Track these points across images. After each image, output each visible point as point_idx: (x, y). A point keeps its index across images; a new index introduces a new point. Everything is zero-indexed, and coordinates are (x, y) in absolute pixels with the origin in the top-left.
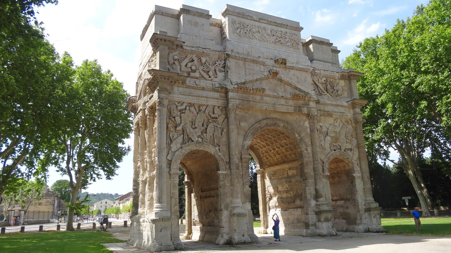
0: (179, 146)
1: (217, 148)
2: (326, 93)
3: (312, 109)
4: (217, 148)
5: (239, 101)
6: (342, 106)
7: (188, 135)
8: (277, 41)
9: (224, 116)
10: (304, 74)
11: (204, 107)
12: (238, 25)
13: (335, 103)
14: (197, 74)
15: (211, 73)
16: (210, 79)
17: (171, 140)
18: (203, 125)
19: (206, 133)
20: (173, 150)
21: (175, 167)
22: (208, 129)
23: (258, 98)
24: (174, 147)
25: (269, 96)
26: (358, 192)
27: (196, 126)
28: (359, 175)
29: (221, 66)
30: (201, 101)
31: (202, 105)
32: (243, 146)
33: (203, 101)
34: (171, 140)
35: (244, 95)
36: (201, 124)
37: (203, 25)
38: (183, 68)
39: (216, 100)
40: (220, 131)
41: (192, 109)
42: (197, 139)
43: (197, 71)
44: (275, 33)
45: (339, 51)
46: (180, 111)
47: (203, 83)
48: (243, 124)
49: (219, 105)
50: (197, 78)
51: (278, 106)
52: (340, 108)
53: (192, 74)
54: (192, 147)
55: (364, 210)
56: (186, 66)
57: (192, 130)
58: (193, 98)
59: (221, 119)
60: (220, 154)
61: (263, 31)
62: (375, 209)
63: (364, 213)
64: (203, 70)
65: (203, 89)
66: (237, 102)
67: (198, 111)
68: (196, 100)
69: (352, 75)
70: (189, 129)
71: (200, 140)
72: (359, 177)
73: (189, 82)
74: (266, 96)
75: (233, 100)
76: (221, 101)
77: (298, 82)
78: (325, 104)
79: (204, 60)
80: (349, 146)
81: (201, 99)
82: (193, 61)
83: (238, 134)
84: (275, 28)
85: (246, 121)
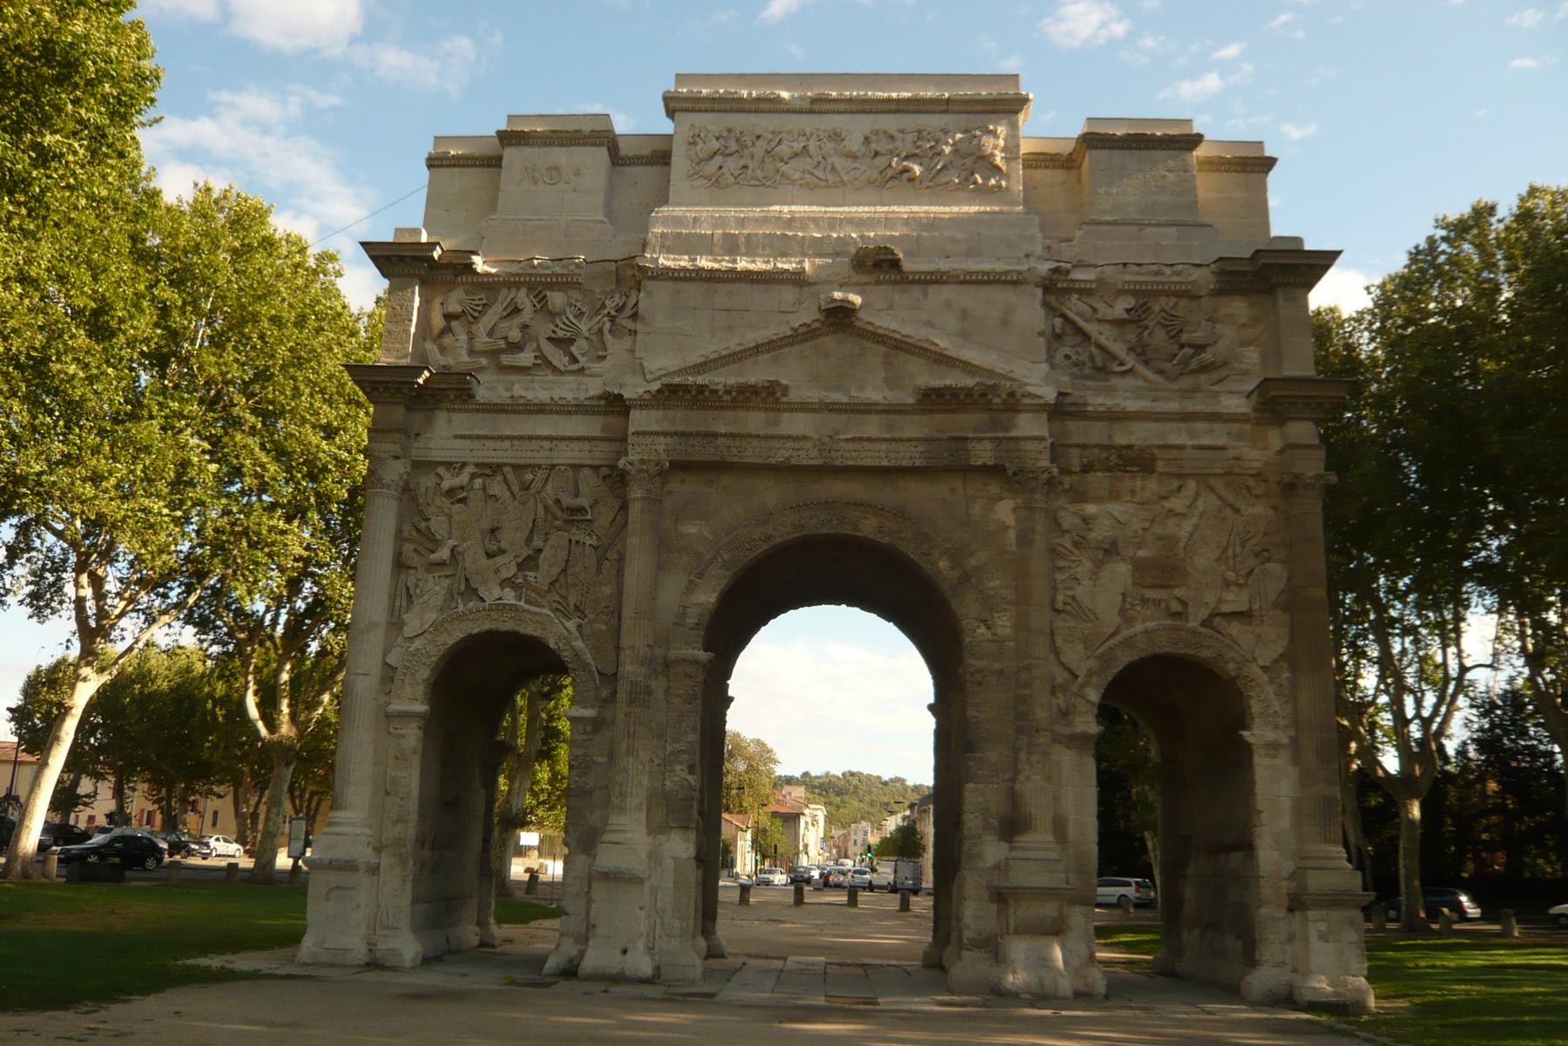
0: (432, 616)
1: (571, 625)
2: (1131, 361)
3: (1030, 446)
4: (571, 625)
5: (669, 440)
8: (890, 173)
9: (616, 504)
10: (1002, 296)
12: (716, 145)
13: (1173, 406)
14: (526, 358)
16: (575, 367)
17: (409, 596)
18: (529, 540)
19: (536, 568)
20: (408, 631)
21: (408, 690)
22: (547, 552)
24: (414, 622)
26: (1263, 816)
27: (503, 545)
28: (1270, 735)
29: (628, 312)
30: (529, 454)
31: (533, 467)
34: (409, 596)
36: (522, 536)
37: (577, 173)
38: (482, 340)
39: (587, 446)
42: (497, 592)
44: (883, 146)
45: (1270, 163)
46: (450, 492)
48: (690, 529)
49: (596, 462)
51: (850, 446)
52: (1200, 426)
53: (506, 360)
55: (1286, 902)
56: (490, 334)
57: (484, 561)
58: (499, 444)
59: (604, 517)
60: (579, 644)
61: (830, 146)
62: (1333, 901)
63: (1282, 913)
64: (549, 339)
65: (540, 409)
67: (516, 489)
69: (1265, 266)
71: (509, 596)
72: (1274, 746)
73: (489, 388)
75: (641, 439)
77: (965, 335)
78: (1116, 417)
80: (1235, 600)
81: (526, 444)
82: (517, 310)
84: (890, 123)
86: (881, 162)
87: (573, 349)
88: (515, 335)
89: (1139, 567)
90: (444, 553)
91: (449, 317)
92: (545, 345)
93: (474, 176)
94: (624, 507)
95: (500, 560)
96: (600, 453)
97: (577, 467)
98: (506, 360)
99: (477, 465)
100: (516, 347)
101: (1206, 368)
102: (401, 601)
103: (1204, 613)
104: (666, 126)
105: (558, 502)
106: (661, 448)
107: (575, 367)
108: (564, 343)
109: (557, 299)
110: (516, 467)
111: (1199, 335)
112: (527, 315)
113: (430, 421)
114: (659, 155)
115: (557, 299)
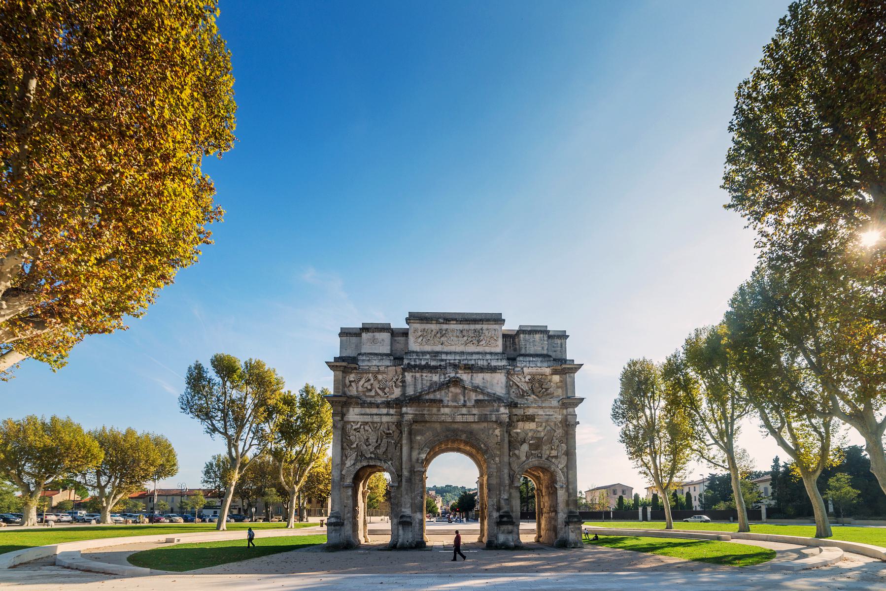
0: (352, 462)
6: (551, 407)
14: (373, 393)
15: (387, 390)
20: (347, 466)
23: (435, 410)
24: (349, 463)
25: (447, 406)
31: (377, 423)
32: (418, 459)
33: (376, 419)
38: (360, 389)
41: (367, 428)
43: (373, 391)
46: (355, 430)
47: (379, 400)
48: (419, 438)
50: (372, 397)
53: (367, 394)
54: (365, 464)
59: (396, 434)
66: (410, 417)
74: (443, 407)
79: (380, 377)
82: (369, 380)
83: (411, 449)
84: (466, 327)
85: (422, 435)
86: (465, 338)
88: (369, 387)
89: (530, 445)
90: (355, 446)
91: (350, 382)
92: (378, 390)
93: (354, 339)
94: (401, 433)
95: (370, 447)
96: (394, 419)
98: (367, 394)
100: (371, 390)
101: (548, 394)
102: (344, 458)
103: (546, 456)
104: (408, 327)
111: (546, 387)
112: (372, 381)
113: (348, 411)
114: (405, 333)
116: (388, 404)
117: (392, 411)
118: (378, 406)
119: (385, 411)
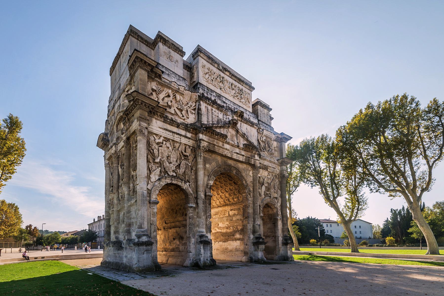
5: (207, 143)
7: (164, 169)
11: (178, 145)
15: (184, 112)
18: (177, 161)
22: (181, 165)
27: (171, 161)
35: (210, 139)
36: (175, 160)
39: (188, 140)
40: (190, 169)
54: (169, 181)
68: (171, 136)
70: (166, 164)
76: (191, 141)
81: (176, 135)
87: (182, 113)
95: (172, 165)
96: (191, 143)
97: (185, 144)
99: (164, 137)
105: (182, 152)
106: (206, 145)
107: (183, 118)
108: (181, 110)
109: (178, 97)
110: (173, 141)
115: (178, 97)
116: (186, 127)
117: (189, 135)
118: (178, 126)
119: (183, 132)
